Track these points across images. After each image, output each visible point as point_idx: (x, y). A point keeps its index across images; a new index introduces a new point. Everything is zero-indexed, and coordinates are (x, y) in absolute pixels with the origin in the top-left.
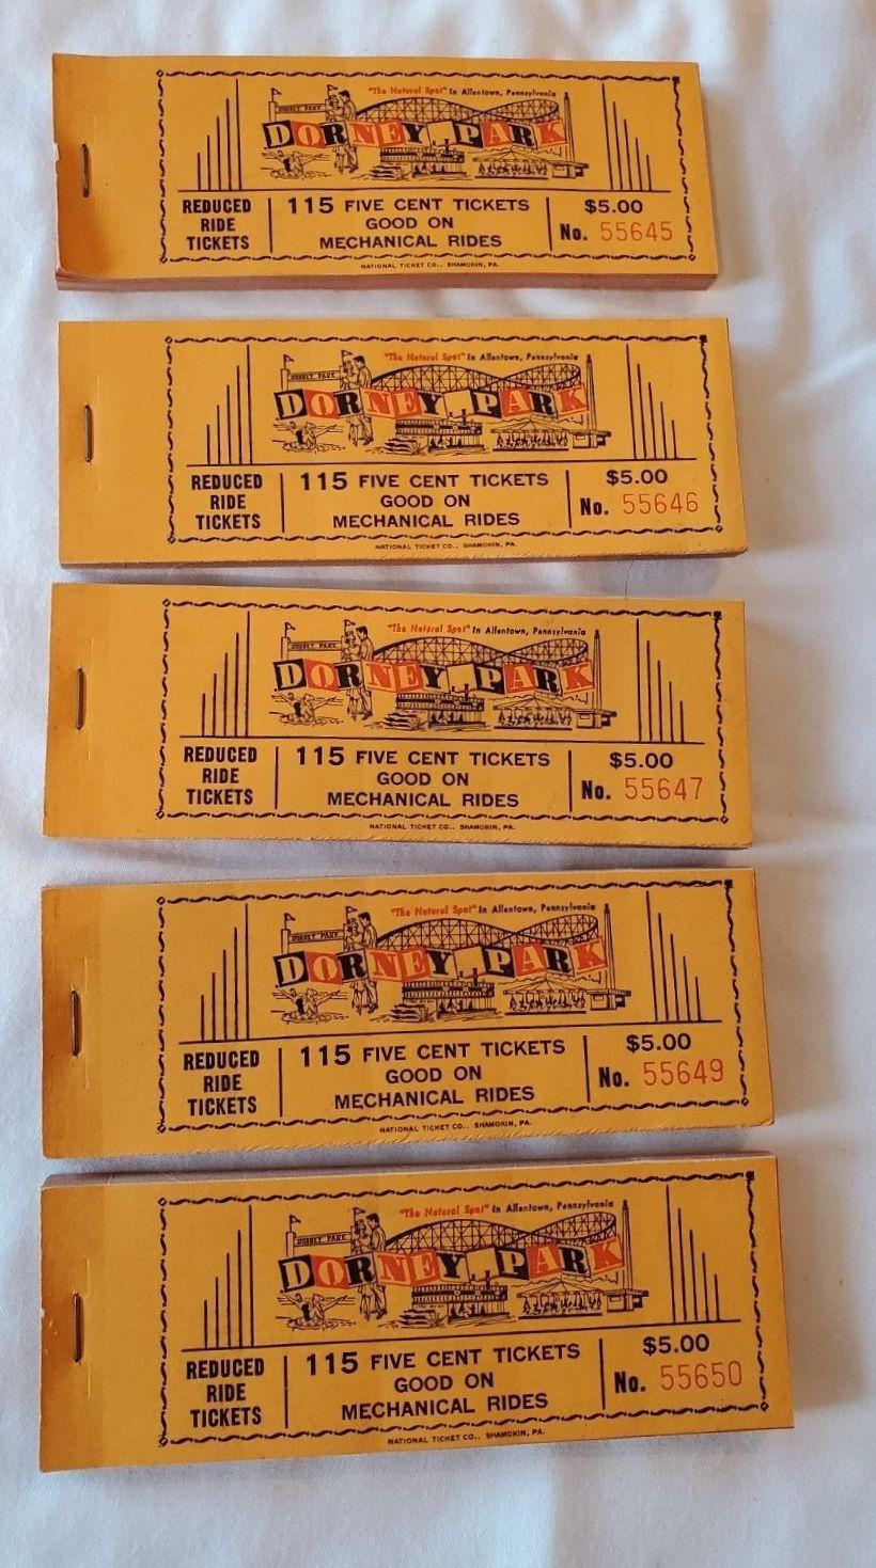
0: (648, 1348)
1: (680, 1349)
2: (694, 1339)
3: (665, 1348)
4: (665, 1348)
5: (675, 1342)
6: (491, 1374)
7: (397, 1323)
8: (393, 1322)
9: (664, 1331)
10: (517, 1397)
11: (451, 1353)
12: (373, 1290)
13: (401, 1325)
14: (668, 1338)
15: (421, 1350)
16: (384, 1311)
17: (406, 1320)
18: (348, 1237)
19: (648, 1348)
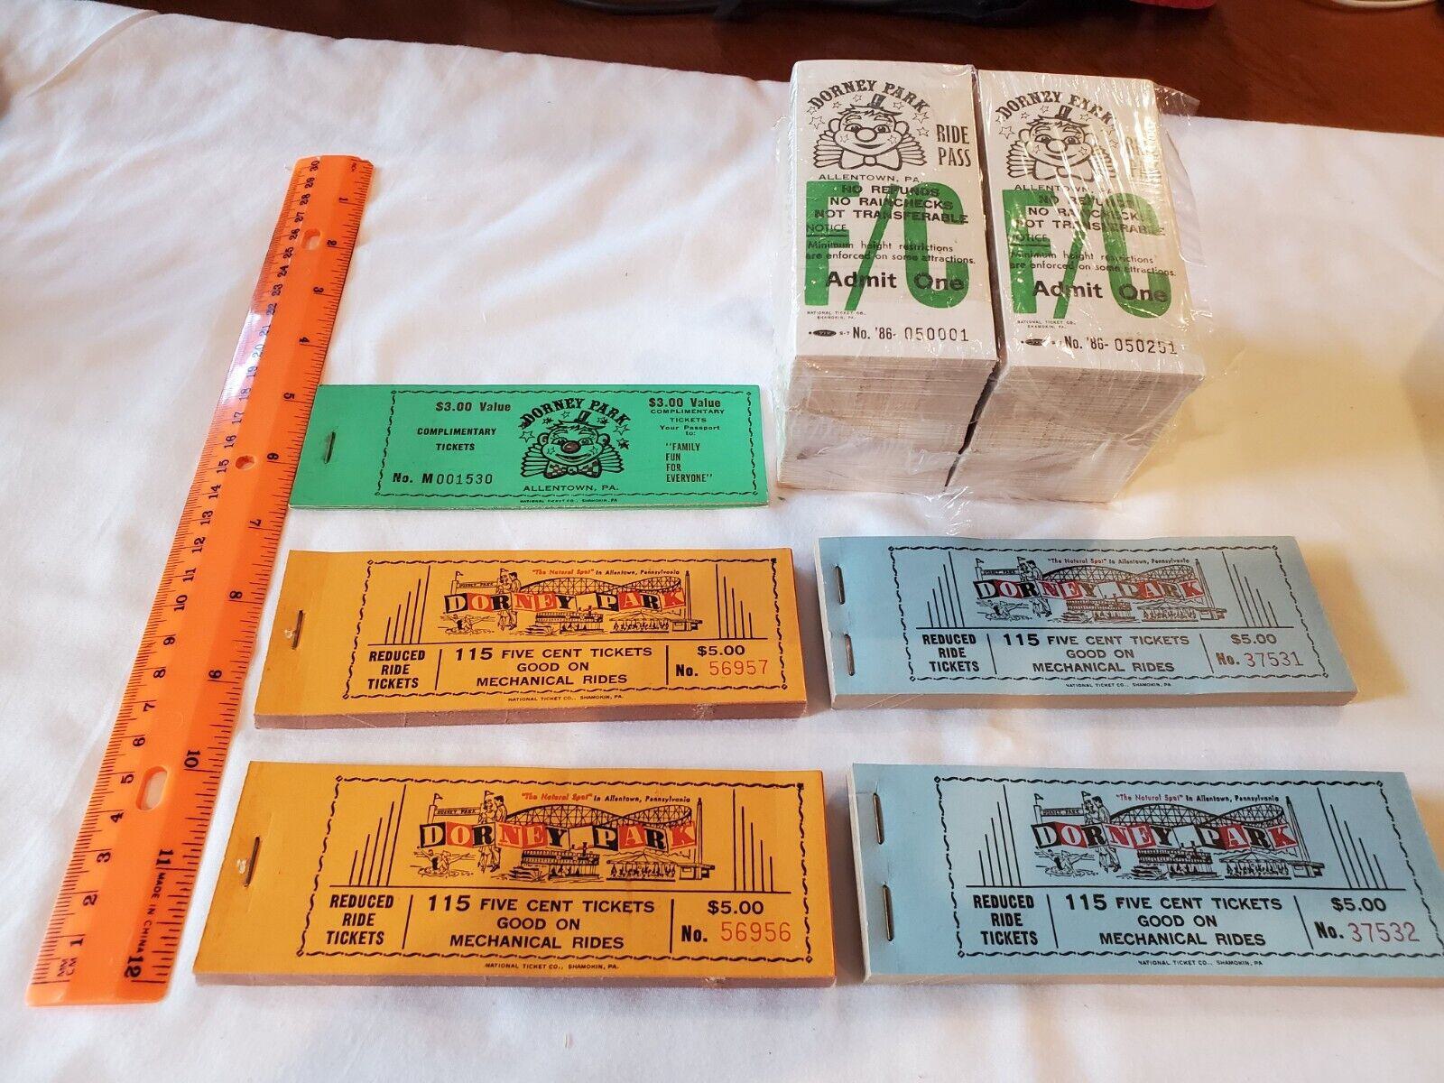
0: (711, 909)
1: (739, 911)
2: (751, 910)
3: (726, 909)
4: (726, 909)
5: (735, 906)
6: (578, 921)
7: (506, 876)
8: (503, 875)
9: (726, 897)
10: (599, 940)
11: (548, 902)
12: (491, 850)
13: (509, 878)
14: (730, 902)
15: (523, 898)
16: (498, 867)
17: (515, 874)
18: (477, 811)
19: (711, 909)
